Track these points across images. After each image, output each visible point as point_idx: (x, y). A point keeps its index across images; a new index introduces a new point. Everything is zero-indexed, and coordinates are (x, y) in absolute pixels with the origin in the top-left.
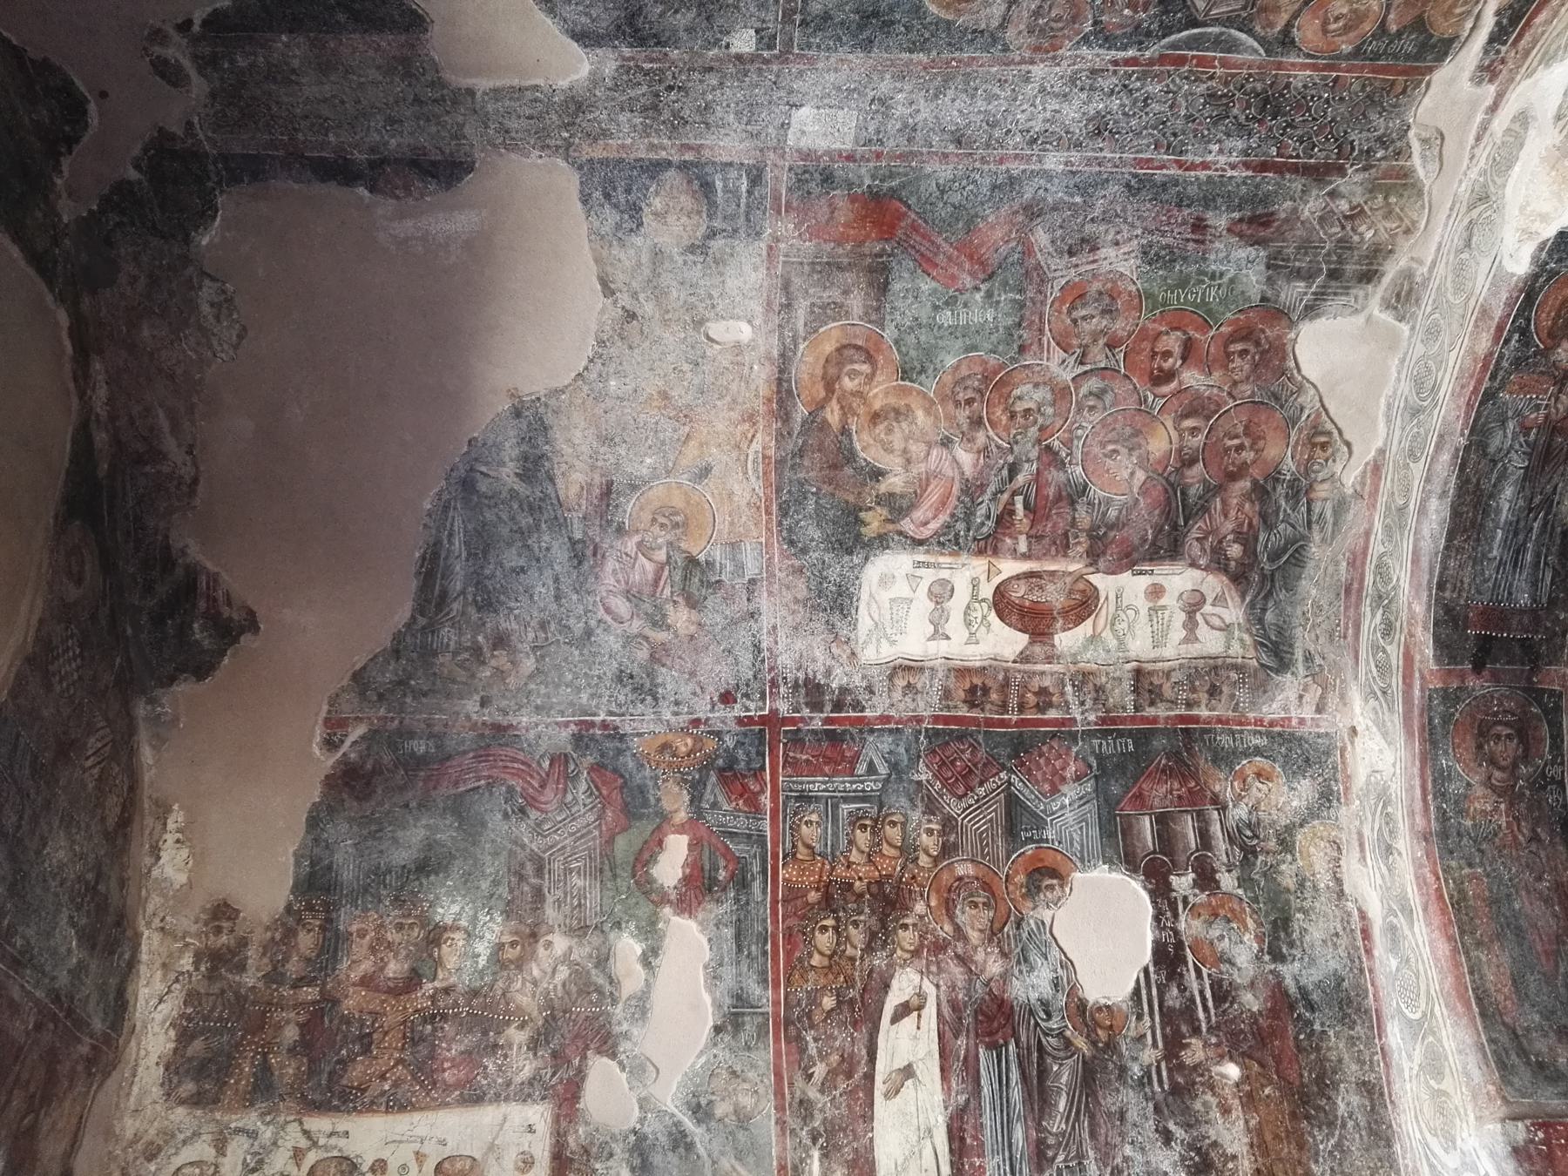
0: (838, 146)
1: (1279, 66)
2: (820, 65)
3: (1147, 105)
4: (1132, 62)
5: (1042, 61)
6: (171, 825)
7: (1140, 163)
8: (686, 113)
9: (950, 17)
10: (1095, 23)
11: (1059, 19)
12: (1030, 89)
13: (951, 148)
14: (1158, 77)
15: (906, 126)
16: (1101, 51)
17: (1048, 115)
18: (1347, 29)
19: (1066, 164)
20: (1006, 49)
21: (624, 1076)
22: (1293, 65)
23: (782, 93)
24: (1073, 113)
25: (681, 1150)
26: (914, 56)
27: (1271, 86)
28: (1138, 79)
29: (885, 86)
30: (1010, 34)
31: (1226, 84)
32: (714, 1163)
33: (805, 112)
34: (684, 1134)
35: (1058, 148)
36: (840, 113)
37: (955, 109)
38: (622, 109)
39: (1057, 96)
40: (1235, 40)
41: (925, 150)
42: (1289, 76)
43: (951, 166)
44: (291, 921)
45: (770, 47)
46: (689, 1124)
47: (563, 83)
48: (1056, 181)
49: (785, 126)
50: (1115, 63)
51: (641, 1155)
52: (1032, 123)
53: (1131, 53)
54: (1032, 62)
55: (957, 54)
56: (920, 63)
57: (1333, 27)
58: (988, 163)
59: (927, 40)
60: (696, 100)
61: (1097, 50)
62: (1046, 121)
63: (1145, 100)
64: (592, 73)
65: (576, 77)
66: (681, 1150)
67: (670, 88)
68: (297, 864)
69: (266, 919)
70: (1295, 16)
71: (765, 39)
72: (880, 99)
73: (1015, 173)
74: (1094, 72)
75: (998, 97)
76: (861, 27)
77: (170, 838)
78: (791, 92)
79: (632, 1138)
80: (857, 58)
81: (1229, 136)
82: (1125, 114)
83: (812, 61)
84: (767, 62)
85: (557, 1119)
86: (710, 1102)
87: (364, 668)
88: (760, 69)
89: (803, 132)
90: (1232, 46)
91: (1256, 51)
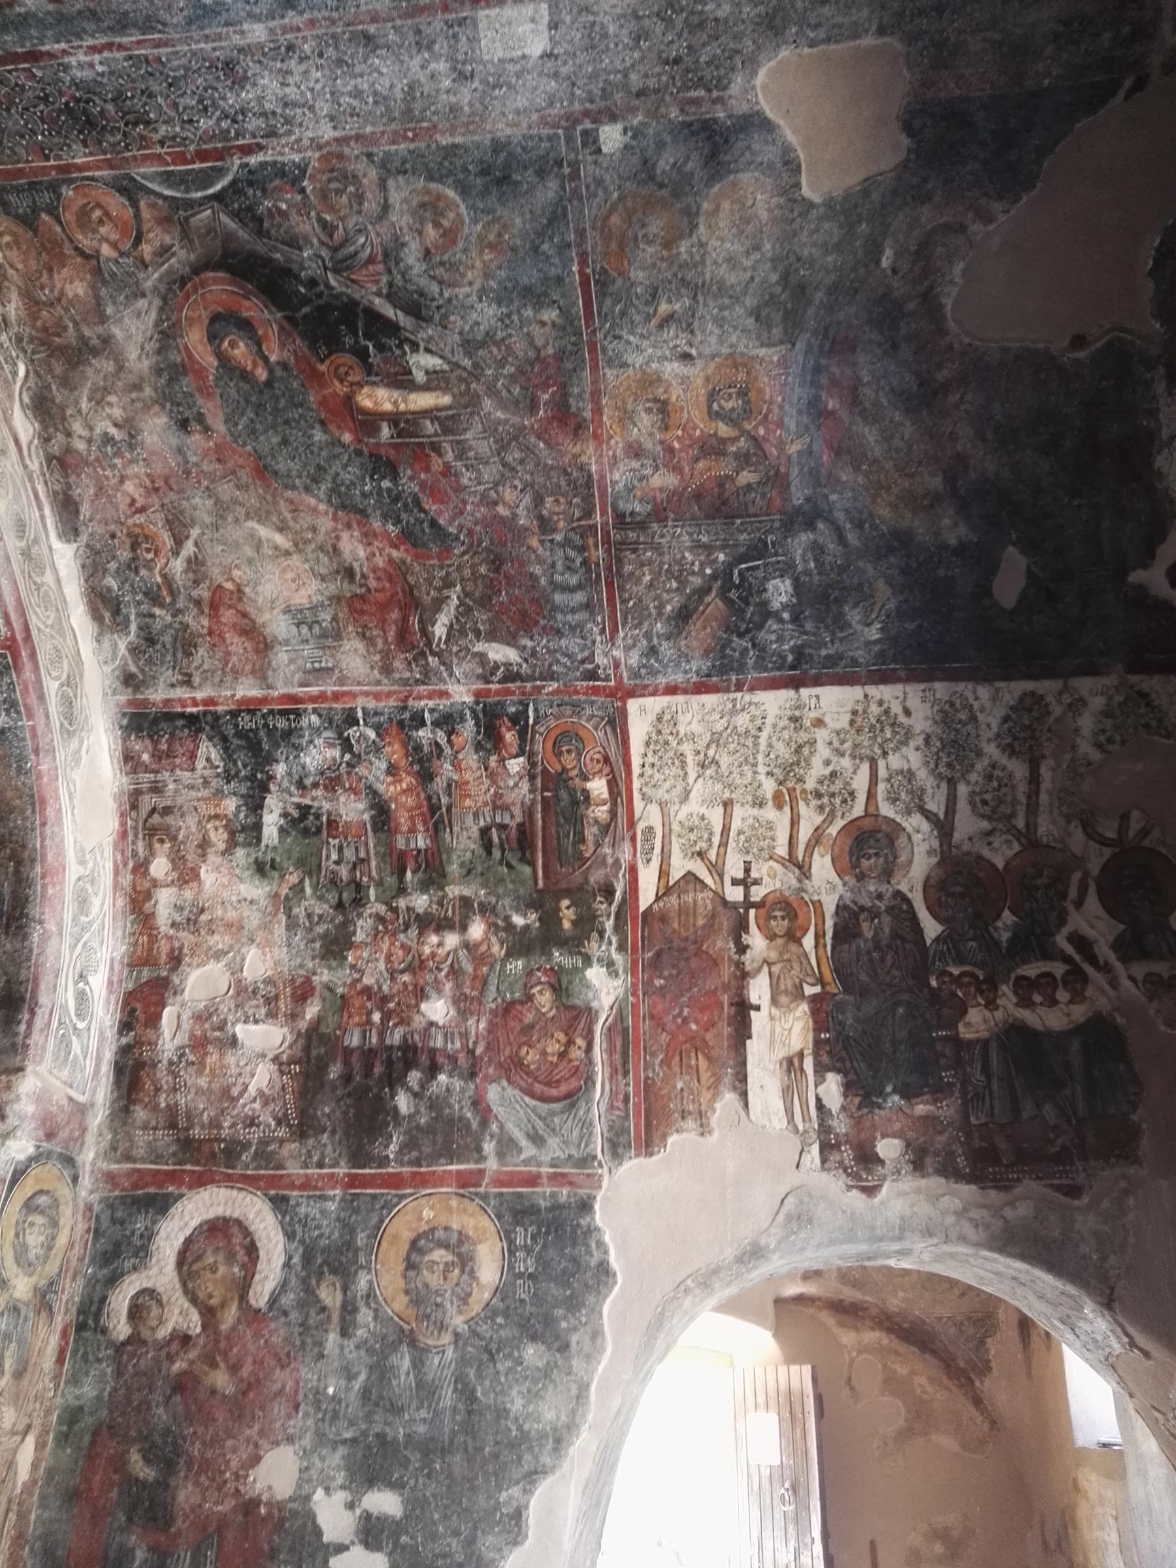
0: (494, 12)
1: (110, 164)
2: (535, 117)
3: (200, 101)
4: (247, 150)
5: (328, 143)
7: (166, 44)
8: (659, 28)
9: (433, 185)
10: (303, 191)
11: (339, 192)
12: (324, 108)
13: (372, 29)
14: (208, 137)
15: (429, 48)
16: (279, 159)
17: (290, 80)
18: (83, 214)
19: (242, 33)
20: (370, 156)
22: (100, 168)
23: (564, 70)
24: (267, 87)
26: (450, 140)
27: (100, 143)
28: (228, 131)
29: (465, 96)
30: (373, 173)
31: (143, 138)
33: (536, 47)
35: (261, 46)
36: (501, 55)
37: (386, 74)
38: (726, 20)
39: (295, 104)
40: (170, 187)
41: (399, 22)
42: (91, 154)
43: (363, 8)
45: (585, 133)
47: (785, 53)
48: (243, 14)
49: (554, 25)
50: (261, 148)
52: (303, 68)
53: (253, 160)
54: (336, 140)
55: (412, 146)
56: (443, 133)
57: (97, 213)
58: (324, 18)
59: (445, 158)
60: (649, 48)
61: (286, 159)
62: (289, 72)
63: (206, 109)
64: (754, 73)
65: (773, 63)
67: (677, 61)
70: (137, 216)
71: (591, 140)
72: (466, 78)
73: (291, 13)
74: (272, 133)
75: (350, 94)
76: (507, 165)
78: (556, 75)
80: (503, 130)
81: (95, 81)
82: (215, 89)
83: (543, 122)
84: (586, 113)
88: (592, 102)
89: (533, 20)
90: (168, 178)
91: (143, 177)
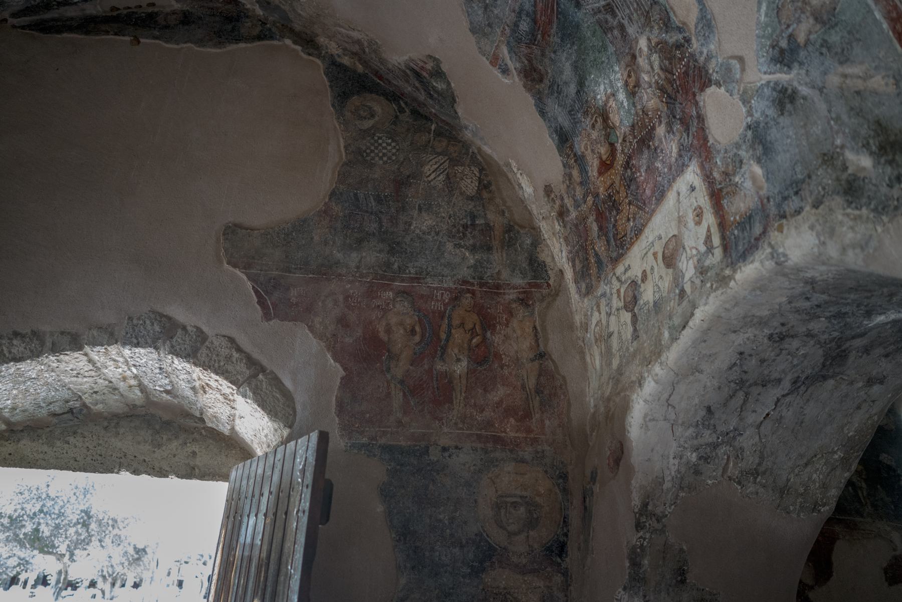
6: (515, 170)
21: (723, 89)
25: (789, 106)
32: (821, 90)
34: (783, 91)
44: (568, 170)
46: (783, 77)
51: (761, 142)
66: (789, 106)
68: (552, 139)
69: (561, 179)
77: (519, 176)
79: (749, 133)
85: (702, 167)
86: (791, 37)
87: (471, 23)
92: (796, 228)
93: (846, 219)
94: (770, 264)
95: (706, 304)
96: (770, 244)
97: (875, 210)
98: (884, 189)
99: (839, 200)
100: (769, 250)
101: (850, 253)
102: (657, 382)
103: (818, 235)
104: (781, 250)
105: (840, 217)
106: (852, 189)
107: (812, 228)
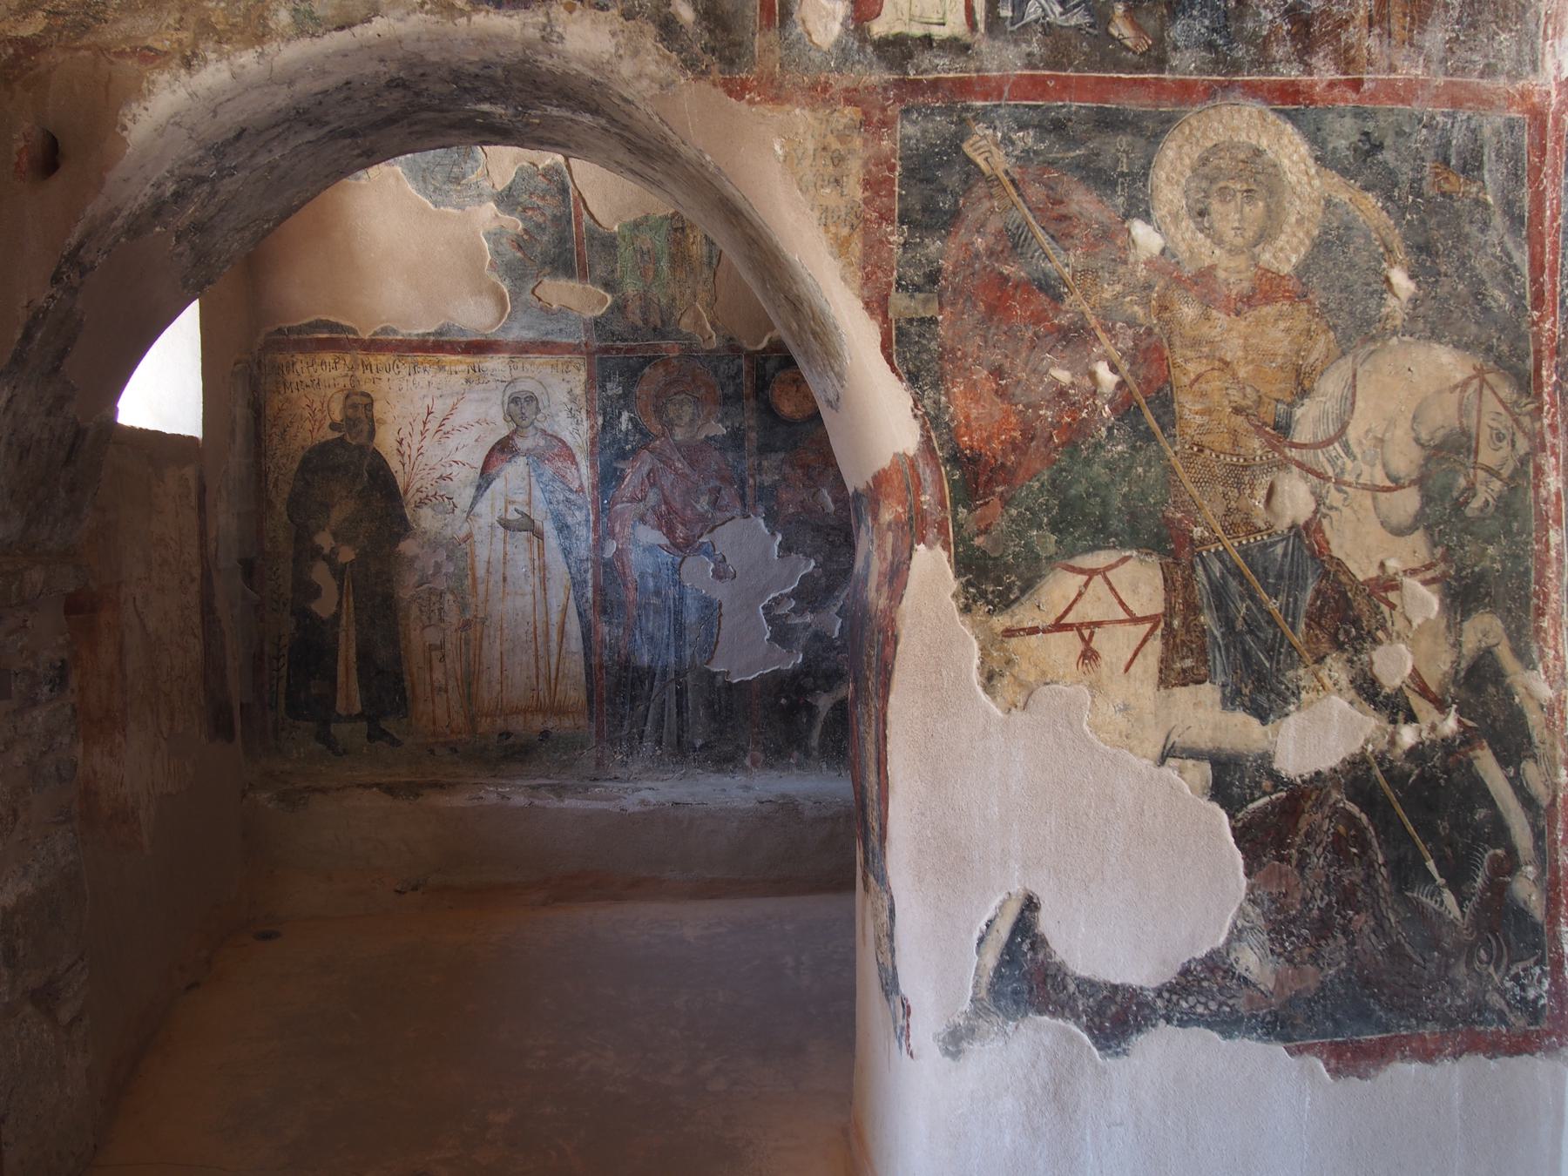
92: (593, 22)
93: (654, 51)
94: (533, 33)
95: (401, 20)
96: (548, 14)
97: (684, 61)
98: (697, 48)
99: (651, 29)
100: (544, 20)
101: (645, 83)
102: (234, 76)
103: (618, 45)
104: (560, 30)
105: (649, 45)
106: (668, 28)
107: (614, 34)
